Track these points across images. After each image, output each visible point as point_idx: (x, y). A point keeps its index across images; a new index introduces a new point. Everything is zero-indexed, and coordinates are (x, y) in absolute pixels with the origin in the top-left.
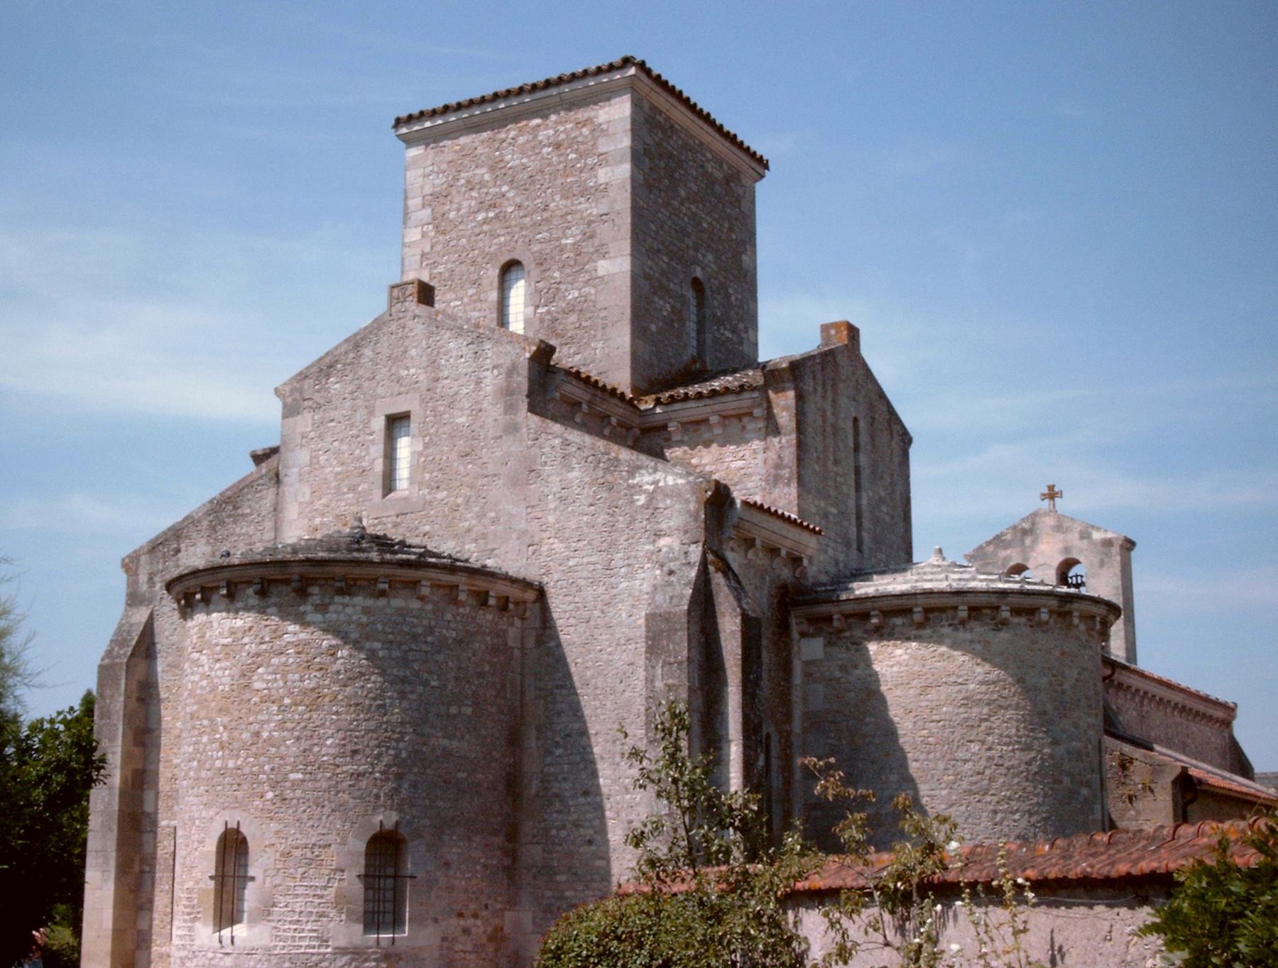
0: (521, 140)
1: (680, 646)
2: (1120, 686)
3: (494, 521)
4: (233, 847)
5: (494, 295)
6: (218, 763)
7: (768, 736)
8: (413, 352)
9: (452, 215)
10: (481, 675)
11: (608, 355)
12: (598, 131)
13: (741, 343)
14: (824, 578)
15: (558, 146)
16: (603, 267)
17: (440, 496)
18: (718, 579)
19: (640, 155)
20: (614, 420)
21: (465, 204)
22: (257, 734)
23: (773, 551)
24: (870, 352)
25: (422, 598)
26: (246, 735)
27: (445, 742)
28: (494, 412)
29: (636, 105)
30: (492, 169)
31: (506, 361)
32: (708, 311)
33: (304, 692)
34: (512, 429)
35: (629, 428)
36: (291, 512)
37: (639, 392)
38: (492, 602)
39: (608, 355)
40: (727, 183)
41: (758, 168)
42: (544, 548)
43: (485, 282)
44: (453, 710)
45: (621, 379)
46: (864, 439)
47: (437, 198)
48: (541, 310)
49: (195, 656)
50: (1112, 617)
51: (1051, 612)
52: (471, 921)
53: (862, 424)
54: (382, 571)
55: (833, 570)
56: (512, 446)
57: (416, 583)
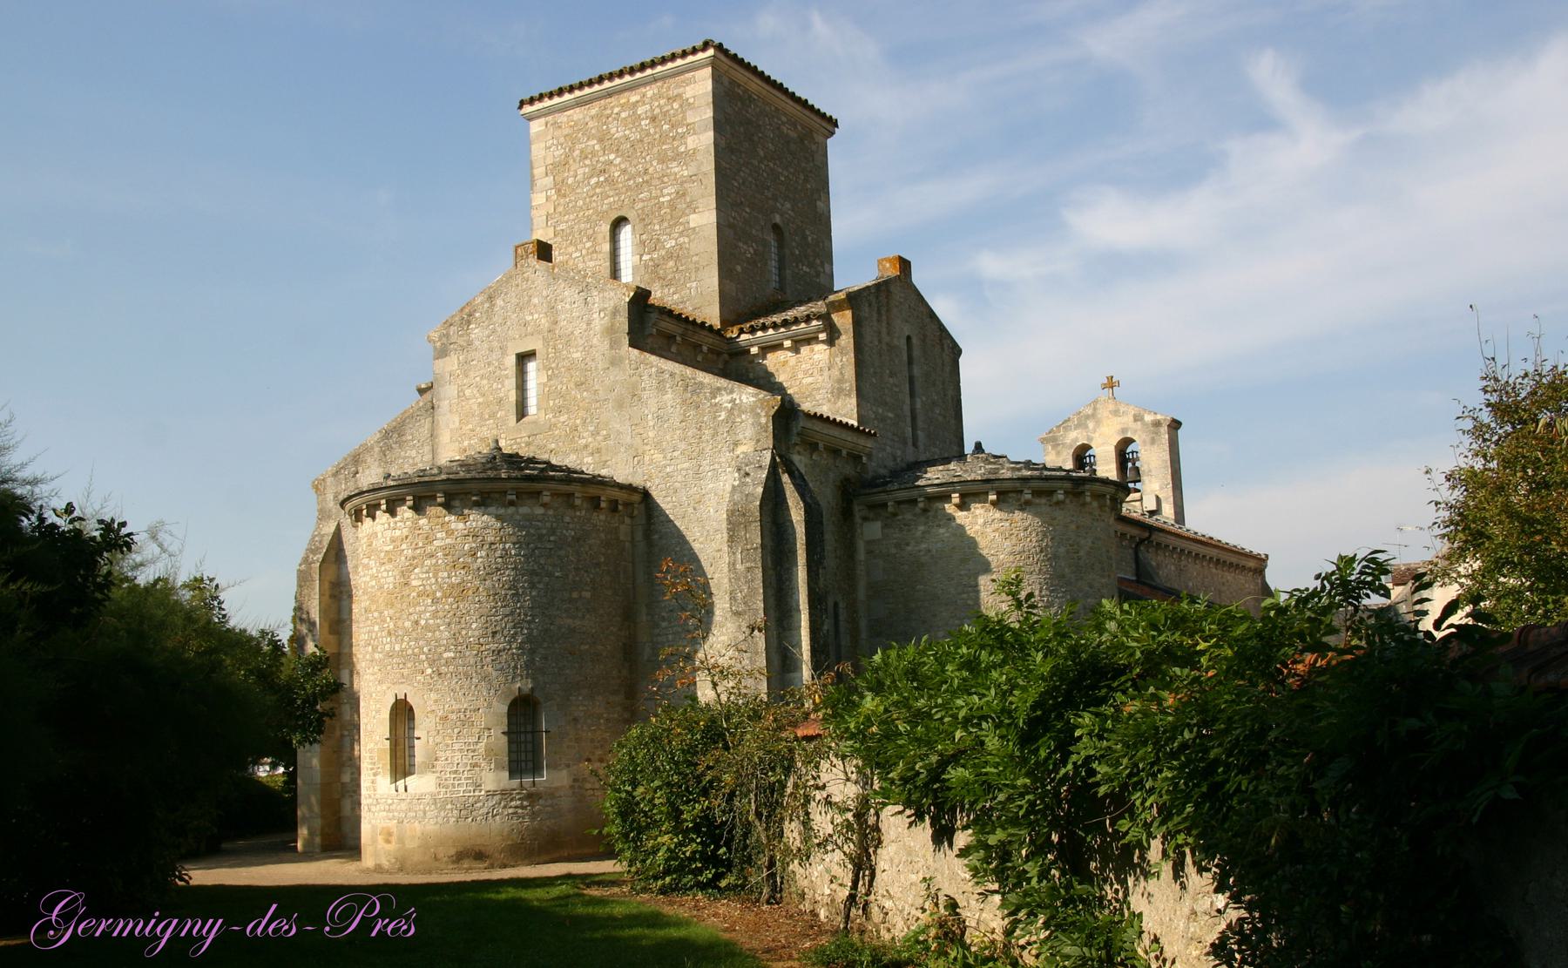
0: (623, 115)
1: (755, 536)
2: (1158, 544)
3: (606, 438)
4: (402, 713)
5: (606, 247)
6: (387, 647)
7: (836, 605)
8: (535, 301)
9: (570, 181)
10: (598, 565)
11: (698, 294)
12: (686, 105)
13: (818, 275)
14: (882, 471)
15: (653, 119)
16: (694, 220)
17: (562, 419)
18: (785, 478)
19: (719, 125)
20: (705, 349)
22: (417, 623)
23: (835, 452)
24: (917, 278)
25: (544, 505)
26: (408, 624)
27: (569, 621)
28: (601, 345)
29: (716, 79)
30: (601, 141)
31: (610, 305)
32: (787, 251)
33: (452, 586)
34: (615, 362)
35: (719, 354)
36: (445, 437)
37: (726, 323)
38: (603, 505)
39: (698, 294)
40: (802, 141)
41: (830, 128)
42: (647, 458)
43: (600, 237)
44: (575, 595)
45: (711, 314)
46: (916, 353)
47: (557, 168)
48: (645, 257)
49: (366, 561)
50: (1121, 495)
51: (1066, 493)
52: (597, 764)
53: (914, 341)
54: (509, 485)
55: (891, 464)
56: (616, 375)
57: (539, 493)
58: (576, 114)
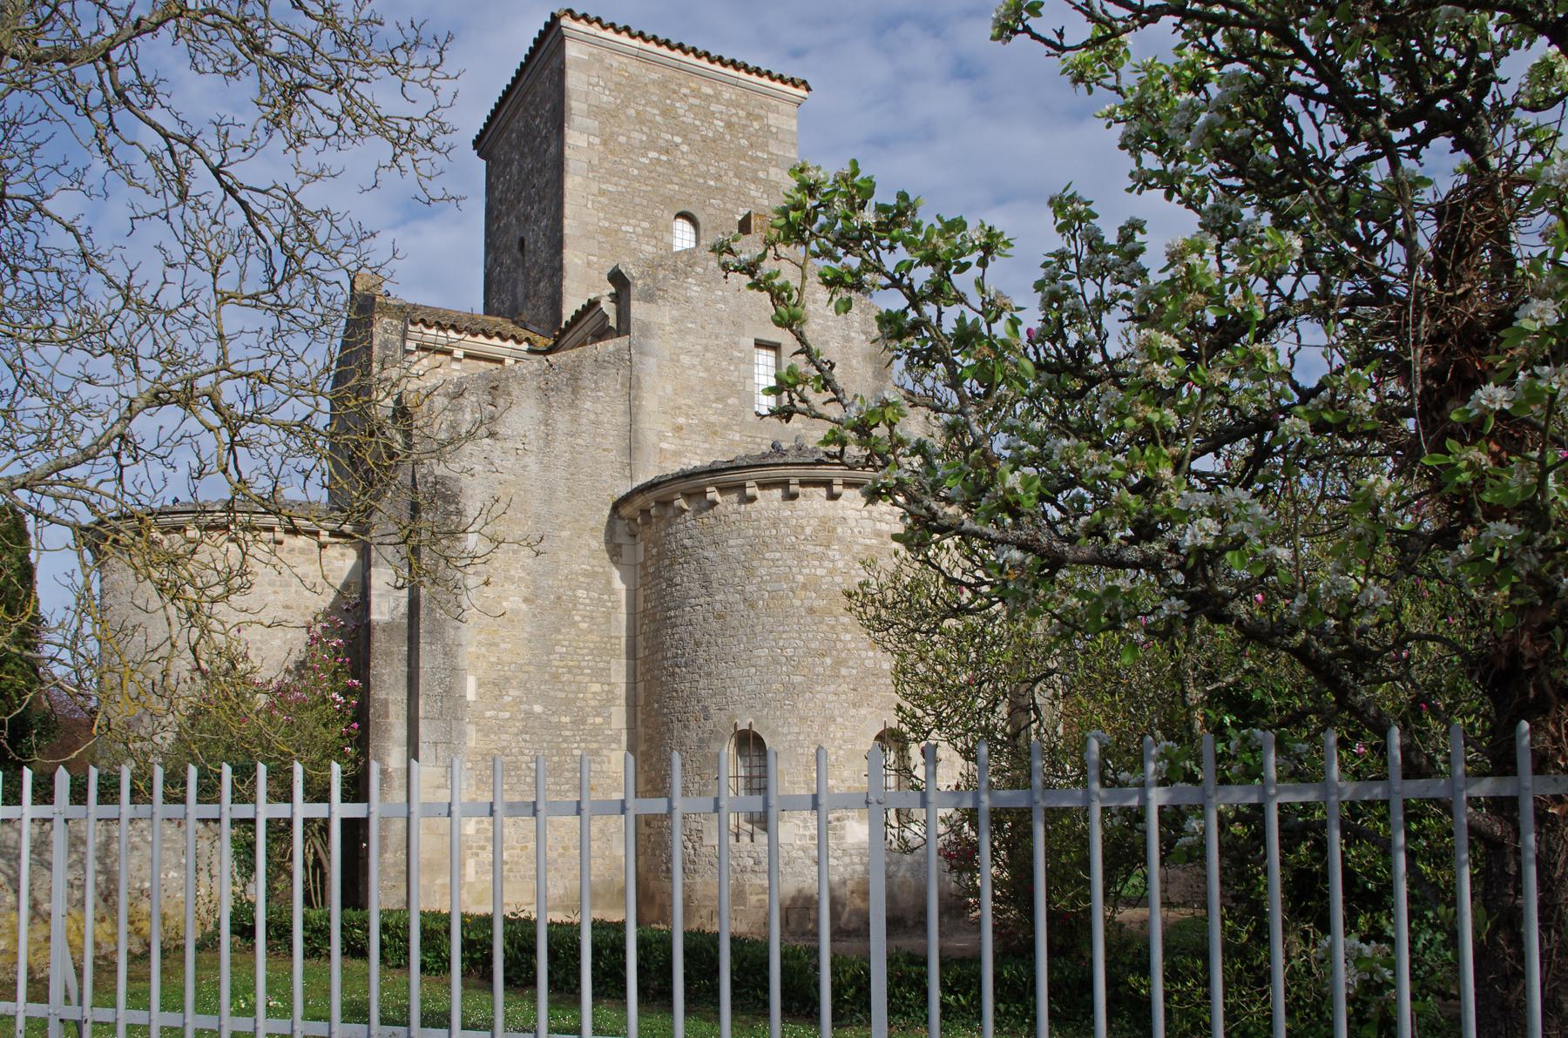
0: (692, 100)
15: (729, 125)
21: (635, 135)
30: (664, 114)
58: (634, 67)
